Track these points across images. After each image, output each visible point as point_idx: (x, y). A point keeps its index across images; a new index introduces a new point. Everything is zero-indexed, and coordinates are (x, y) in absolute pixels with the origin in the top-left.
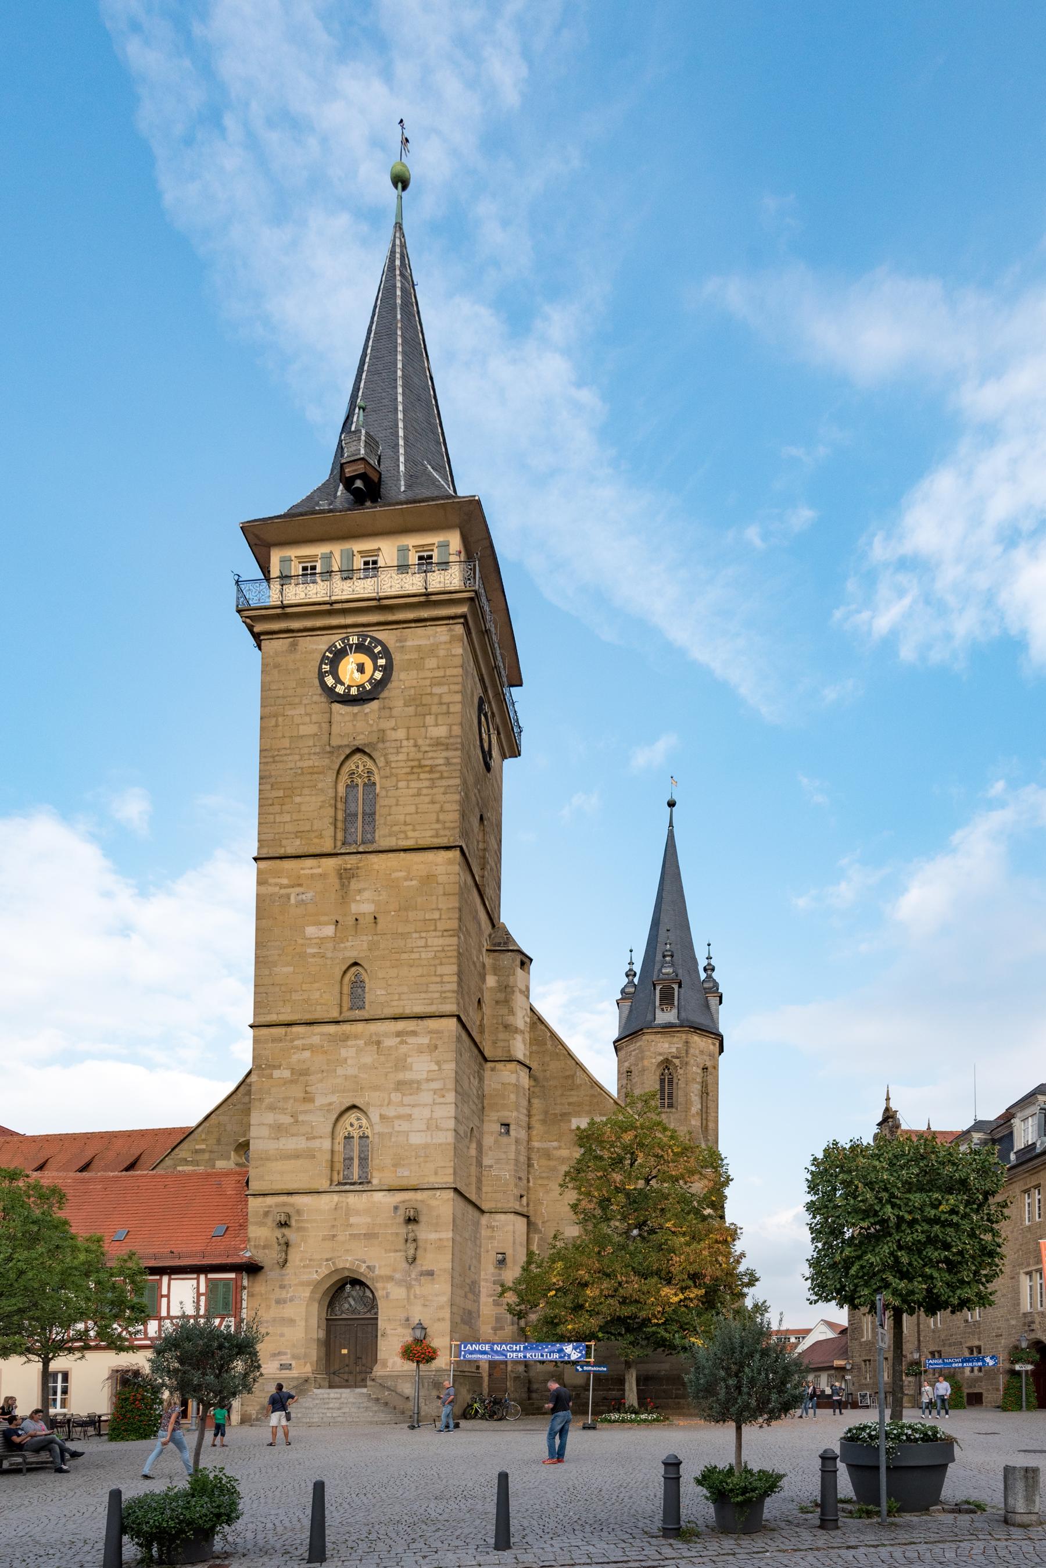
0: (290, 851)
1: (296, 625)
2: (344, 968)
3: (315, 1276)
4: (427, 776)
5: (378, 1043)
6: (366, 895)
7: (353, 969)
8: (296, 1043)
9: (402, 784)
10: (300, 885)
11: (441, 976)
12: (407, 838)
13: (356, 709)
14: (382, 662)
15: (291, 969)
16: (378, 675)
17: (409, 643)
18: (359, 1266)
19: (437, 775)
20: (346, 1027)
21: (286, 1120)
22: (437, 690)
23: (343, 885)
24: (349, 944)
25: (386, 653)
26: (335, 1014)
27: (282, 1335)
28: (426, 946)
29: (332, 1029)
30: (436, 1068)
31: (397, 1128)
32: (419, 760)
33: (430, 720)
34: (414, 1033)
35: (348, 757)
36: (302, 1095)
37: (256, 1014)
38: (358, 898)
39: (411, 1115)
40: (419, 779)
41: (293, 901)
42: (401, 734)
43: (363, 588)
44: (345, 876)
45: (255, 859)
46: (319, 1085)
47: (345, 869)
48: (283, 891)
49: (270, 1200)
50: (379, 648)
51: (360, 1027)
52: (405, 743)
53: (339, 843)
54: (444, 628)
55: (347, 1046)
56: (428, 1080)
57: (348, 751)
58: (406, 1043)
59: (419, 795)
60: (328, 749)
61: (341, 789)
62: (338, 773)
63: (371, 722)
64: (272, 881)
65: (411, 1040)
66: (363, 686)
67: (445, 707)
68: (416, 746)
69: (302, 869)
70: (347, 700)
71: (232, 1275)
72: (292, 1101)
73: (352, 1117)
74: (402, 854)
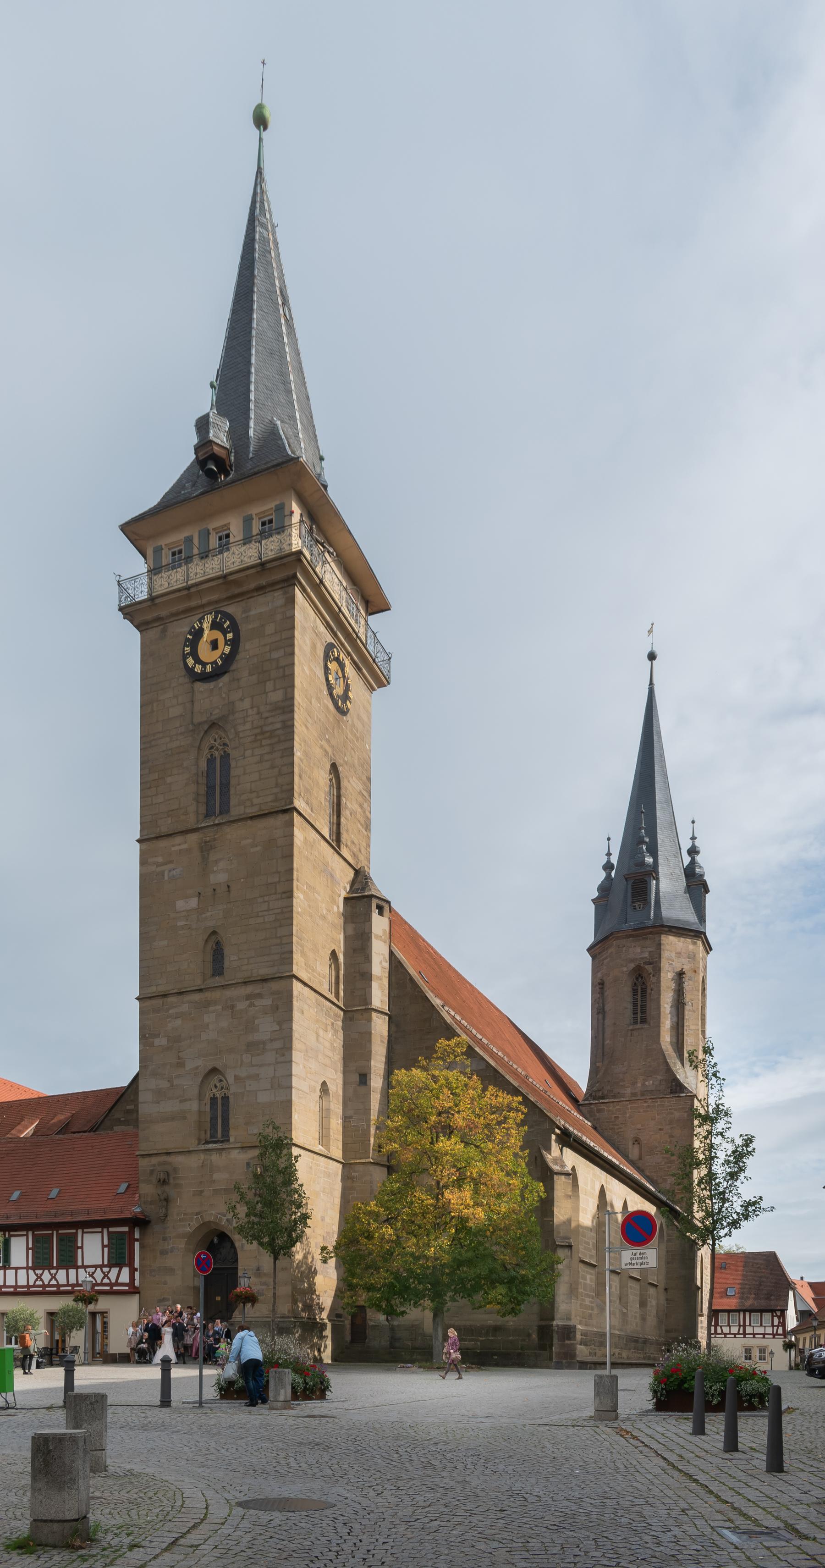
0: (164, 830)
2: (205, 937)
3: (188, 1229)
4: (269, 742)
5: (232, 1007)
6: (222, 865)
7: (213, 938)
8: (170, 1012)
9: (248, 753)
10: (171, 862)
11: (280, 937)
12: (252, 805)
13: (211, 685)
14: (230, 636)
15: (165, 942)
16: (227, 650)
17: (253, 613)
18: (221, 1219)
19: (276, 740)
20: (208, 995)
21: (164, 1084)
22: (275, 655)
24: (209, 914)
25: (234, 628)
26: (198, 982)
27: (165, 1283)
28: (268, 910)
29: (196, 997)
30: (277, 1028)
31: (248, 1089)
32: (261, 727)
33: (269, 686)
34: (260, 996)
35: (206, 732)
37: (141, 987)
38: (215, 869)
39: (258, 1075)
40: (262, 746)
41: (166, 878)
42: (247, 703)
43: (213, 567)
44: (206, 848)
45: (138, 841)
47: (206, 842)
48: (160, 869)
49: (154, 1160)
50: (228, 623)
51: (217, 994)
52: (250, 712)
53: (201, 817)
54: (280, 592)
56: (272, 1040)
57: (206, 727)
58: (254, 1006)
59: (261, 762)
60: (191, 727)
61: (203, 765)
62: (199, 748)
63: (224, 695)
64: (150, 860)
65: (258, 1002)
66: (215, 662)
67: (281, 670)
68: (258, 713)
69: (173, 846)
70: (204, 678)
71: (126, 1229)
73: (215, 1080)
74: (249, 822)
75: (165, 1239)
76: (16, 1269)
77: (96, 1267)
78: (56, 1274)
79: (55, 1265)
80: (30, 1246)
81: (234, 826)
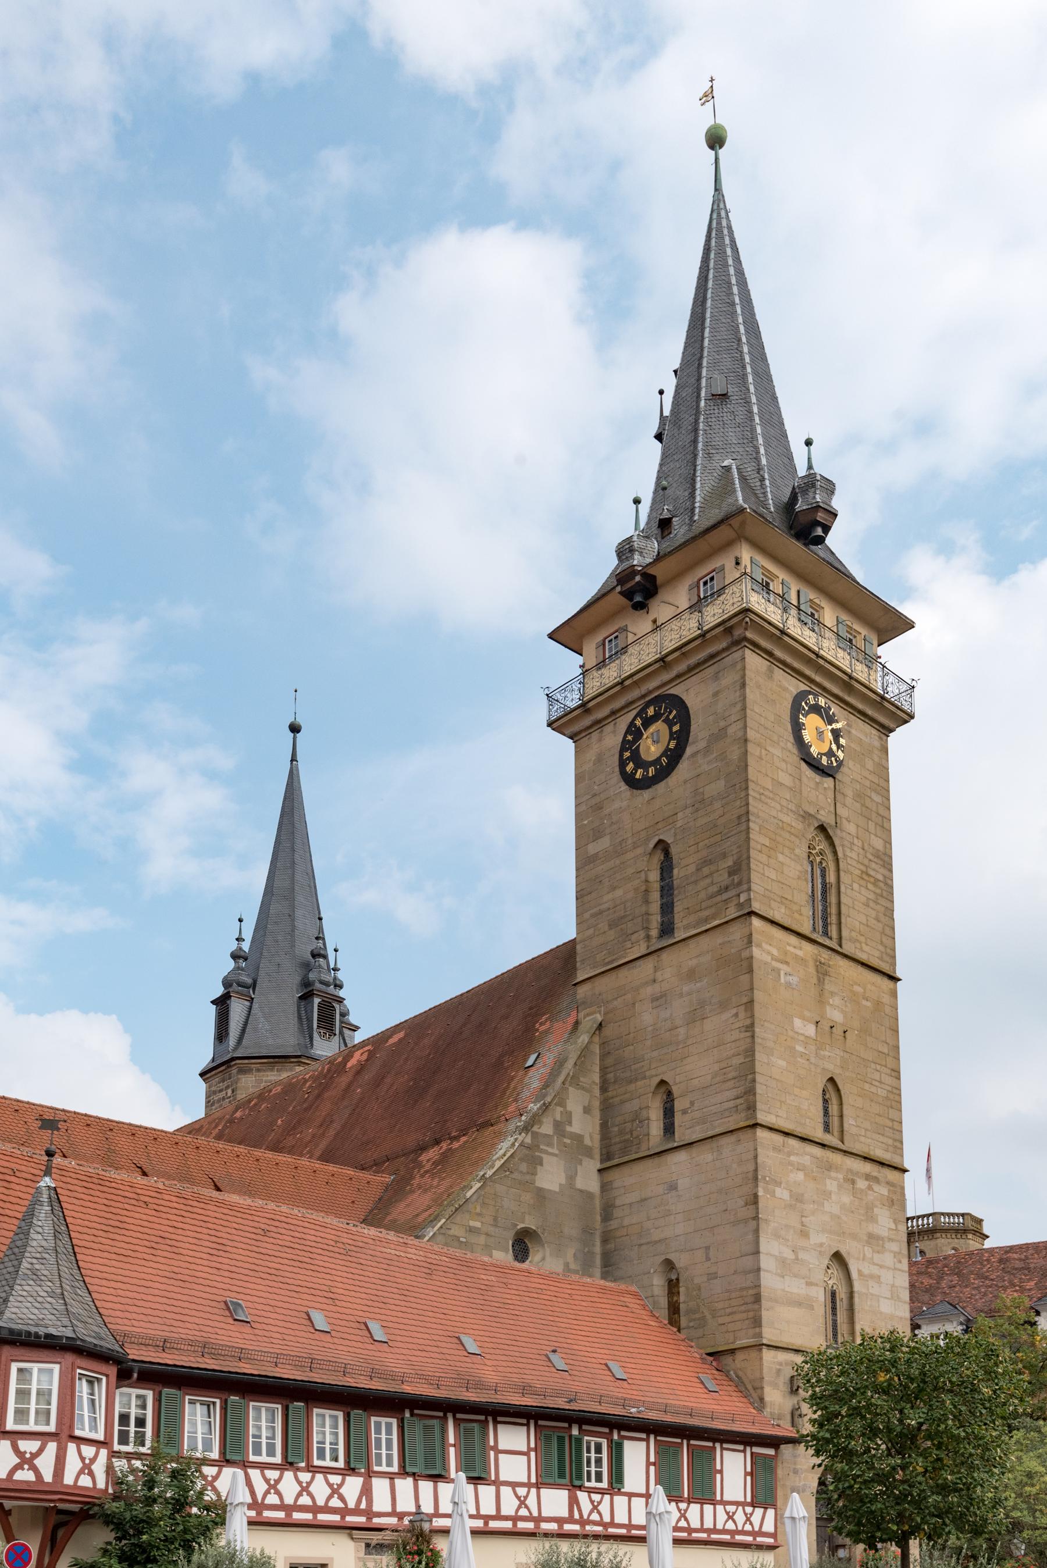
1: (778, 653)
8: (792, 1158)
21: (789, 1255)
23: (819, 980)
36: (799, 1226)
46: (811, 1218)
55: (830, 1178)
69: (789, 944)
72: (792, 1231)
75: (796, 1472)
76: (630, 1495)
77: (737, 1503)
78: (686, 1511)
79: (686, 1495)
80: (652, 1459)
81: (852, 964)
